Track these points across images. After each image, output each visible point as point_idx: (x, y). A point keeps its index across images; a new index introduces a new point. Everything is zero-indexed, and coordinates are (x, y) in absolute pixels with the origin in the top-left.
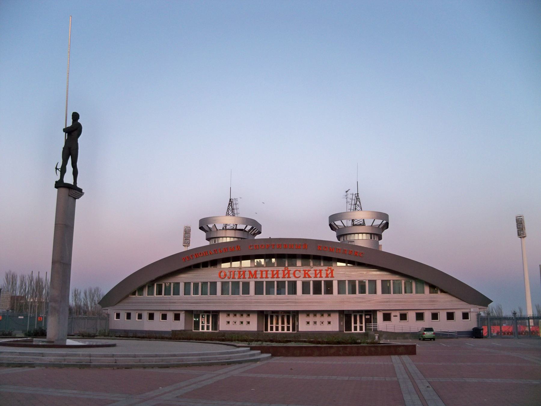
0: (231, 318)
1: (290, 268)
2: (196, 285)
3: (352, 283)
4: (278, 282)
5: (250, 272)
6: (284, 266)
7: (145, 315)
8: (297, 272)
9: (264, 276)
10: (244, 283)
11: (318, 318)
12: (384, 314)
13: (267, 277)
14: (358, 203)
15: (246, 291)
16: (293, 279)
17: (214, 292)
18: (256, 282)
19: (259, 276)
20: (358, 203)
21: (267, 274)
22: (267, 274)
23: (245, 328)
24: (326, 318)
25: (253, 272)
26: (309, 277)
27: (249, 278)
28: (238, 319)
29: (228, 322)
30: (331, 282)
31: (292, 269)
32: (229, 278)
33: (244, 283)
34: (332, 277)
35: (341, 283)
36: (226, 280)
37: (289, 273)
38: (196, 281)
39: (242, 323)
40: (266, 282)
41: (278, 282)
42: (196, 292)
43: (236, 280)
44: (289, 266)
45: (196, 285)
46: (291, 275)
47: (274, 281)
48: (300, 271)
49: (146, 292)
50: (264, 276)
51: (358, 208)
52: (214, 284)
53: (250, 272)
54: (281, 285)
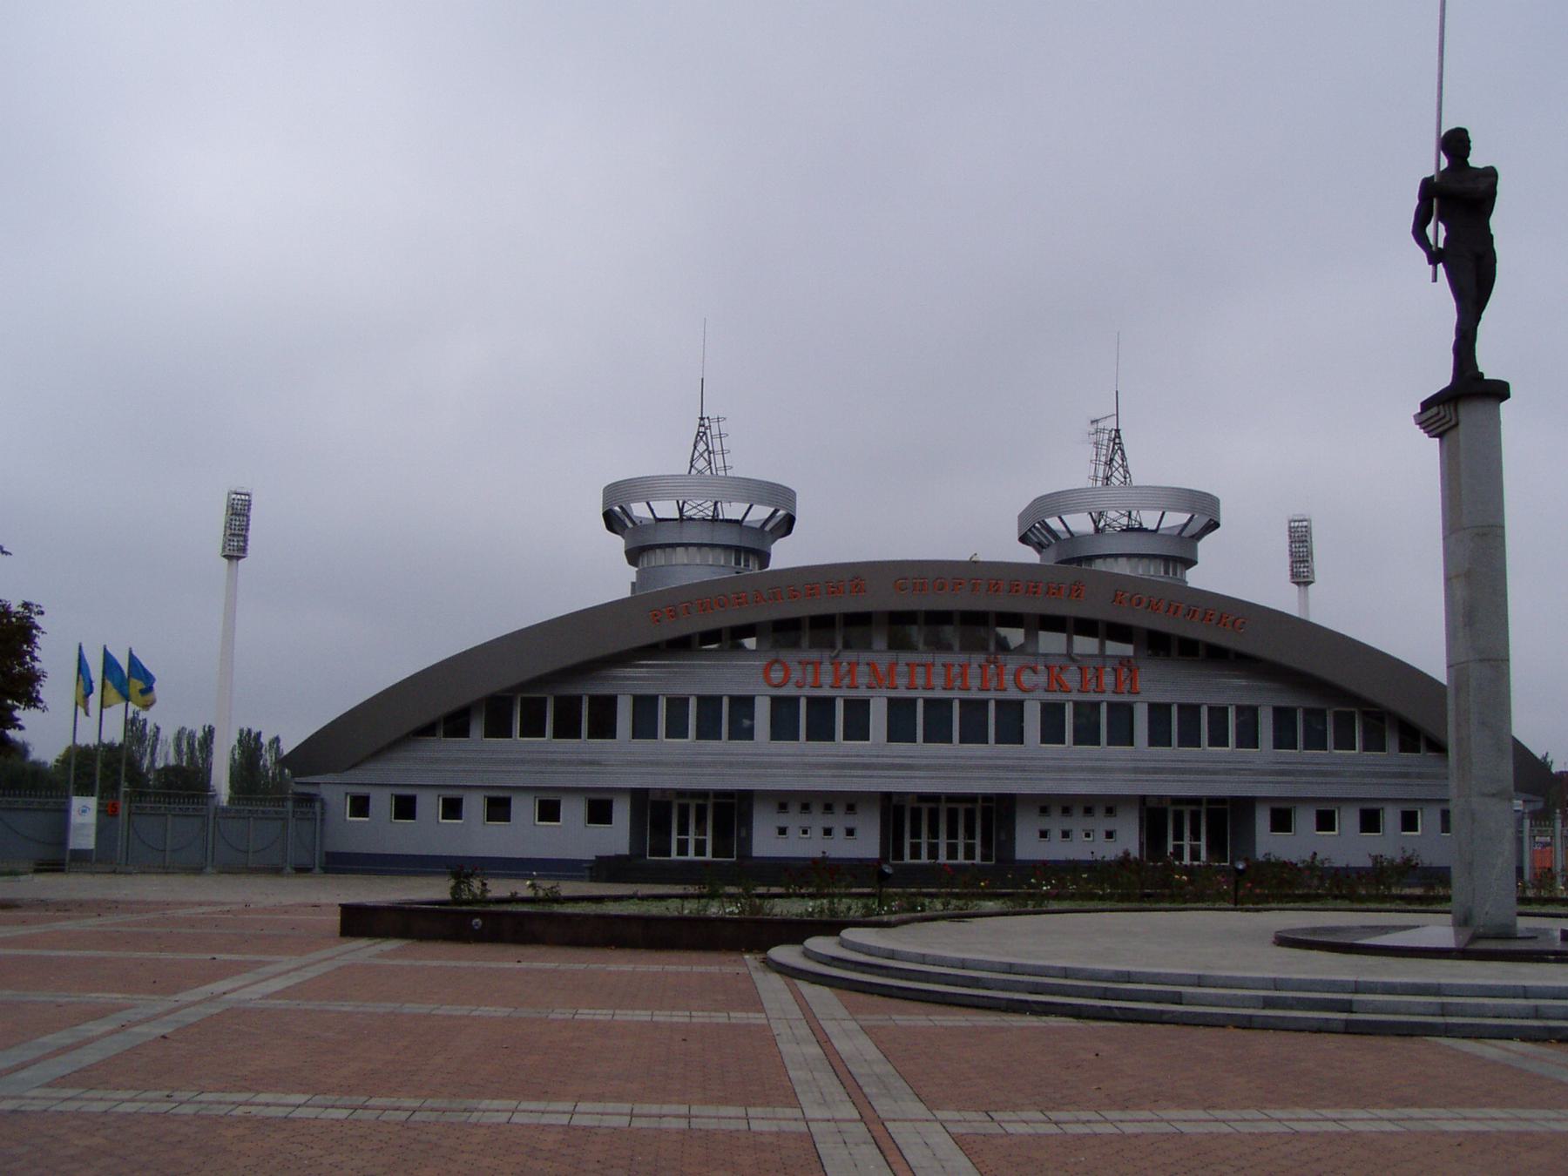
0: (793, 820)
2: (678, 705)
3: (1190, 712)
9: (920, 681)
10: (849, 703)
13: (929, 687)
16: (1012, 694)
17: (742, 732)
18: (890, 700)
23: (841, 848)
27: (870, 687)
28: (818, 821)
29: (782, 831)
30: (1129, 709)
33: (849, 703)
38: (679, 690)
40: (927, 701)
43: (826, 692)
46: (1008, 679)
50: (920, 681)
52: (744, 705)
54: (975, 709)
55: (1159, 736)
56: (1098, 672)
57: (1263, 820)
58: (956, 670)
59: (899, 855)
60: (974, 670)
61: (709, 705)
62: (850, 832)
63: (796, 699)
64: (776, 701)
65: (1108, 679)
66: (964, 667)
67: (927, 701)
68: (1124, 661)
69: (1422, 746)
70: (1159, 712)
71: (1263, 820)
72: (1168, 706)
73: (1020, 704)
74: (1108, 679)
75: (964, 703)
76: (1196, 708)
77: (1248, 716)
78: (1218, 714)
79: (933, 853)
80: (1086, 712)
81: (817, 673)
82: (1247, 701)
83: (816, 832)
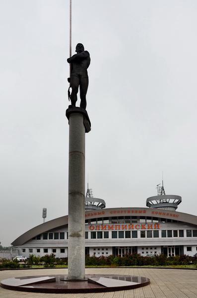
1: (133, 224)
3: (170, 232)
4: (126, 231)
6: (130, 223)
12: (187, 248)
15: (107, 236)
16: (135, 230)
18: (112, 232)
21: (119, 227)
27: (109, 229)
31: (135, 224)
32: (96, 230)
41: (126, 231)
43: (100, 231)
47: (123, 231)
48: (139, 226)
66: (126, 226)
68: (156, 223)
78: (175, 232)
81: (99, 228)
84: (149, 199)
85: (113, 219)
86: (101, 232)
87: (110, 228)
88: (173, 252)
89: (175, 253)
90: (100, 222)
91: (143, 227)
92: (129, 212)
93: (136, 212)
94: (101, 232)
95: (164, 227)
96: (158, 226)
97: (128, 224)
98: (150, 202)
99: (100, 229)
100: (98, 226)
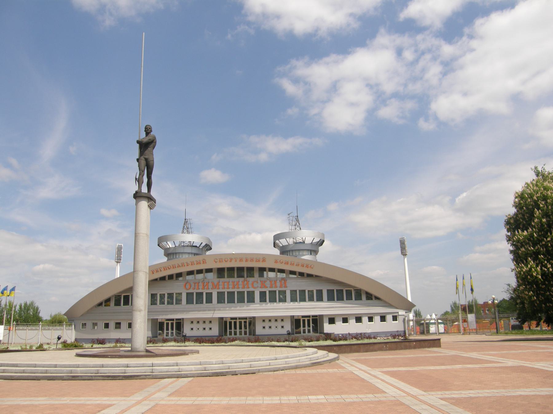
0: (195, 326)
1: (248, 279)
3: (303, 292)
4: (238, 292)
5: (213, 283)
7: (112, 325)
8: (255, 283)
11: (273, 324)
14: (298, 224)
15: (209, 300)
16: (251, 289)
19: (221, 287)
20: (298, 224)
22: (228, 285)
24: (280, 324)
25: (216, 284)
26: (266, 287)
28: (201, 326)
29: (192, 329)
30: (285, 292)
31: (251, 280)
32: (194, 289)
34: (286, 287)
35: (293, 292)
36: (191, 291)
37: (248, 284)
39: (204, 329)
40: (228, 292)
42: (162, 303)
44: (247, 277)
45: (162, 296)
48: (257, 283)
49: (112, 303)
50: (226, 287)
51: (298, 229)
53: (213, 283)
54: (241, 294)
55: (293, 300)
56: (275, 282)
57: (326, 321)
58: (235, 283)
59: (226, 334)
60: (240, 283)
61: (170, 296)
62: (210, 329)
63: (193, 293)
64: (188, 294)
65: (278, 284)
67: (228, 292)
69: (373, 298)
70: (293, 292)
71: (326, 321)
72: (296, 291)
73: (253, 292)
74: (278, 284)
75: (238, 292)
76: (304, 291)
77: (320, 292)
78: (311, 292)
79: (235, 334)
80: (273, 293)
82: (319, 288)
83: (201, 329)
84: (277, 237)
85: (220, 272)
86: (202, 293)
87: (214, 287)
88: (309, 326)
89: (311, 328)
90: (200, 276)
91: (263, 285)
92: (241, 260)
93: (252, 260)
94: (202, 293)
95: (295, 284)
96: (285, 283)
97: (241, 279)
98: (277, 241)
99: (201, 287)
100: (197, 283)
